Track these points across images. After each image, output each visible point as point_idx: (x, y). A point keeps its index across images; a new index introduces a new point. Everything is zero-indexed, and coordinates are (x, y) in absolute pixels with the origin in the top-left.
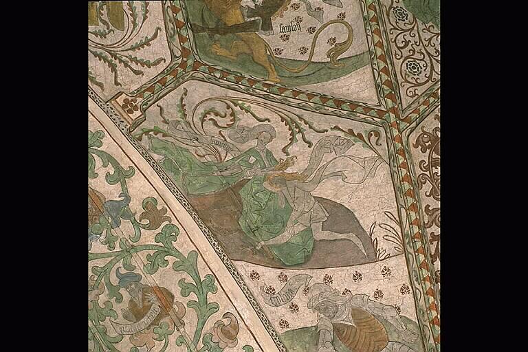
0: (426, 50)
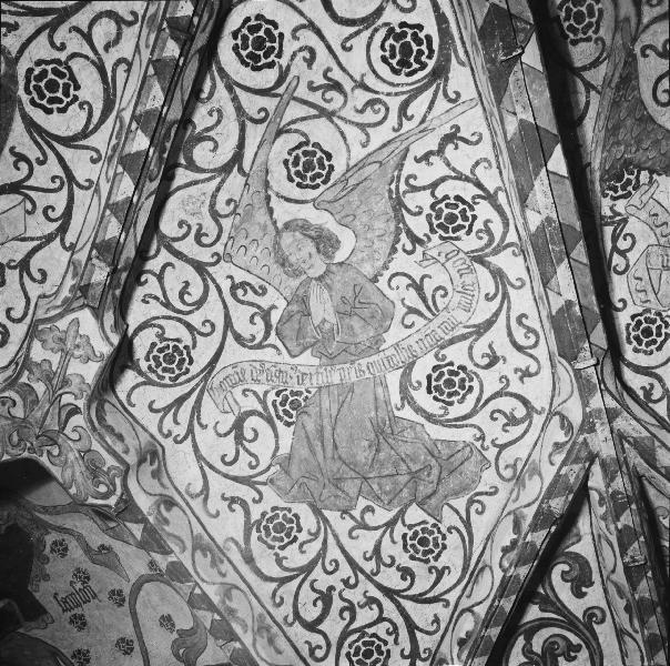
0: (380, 587)
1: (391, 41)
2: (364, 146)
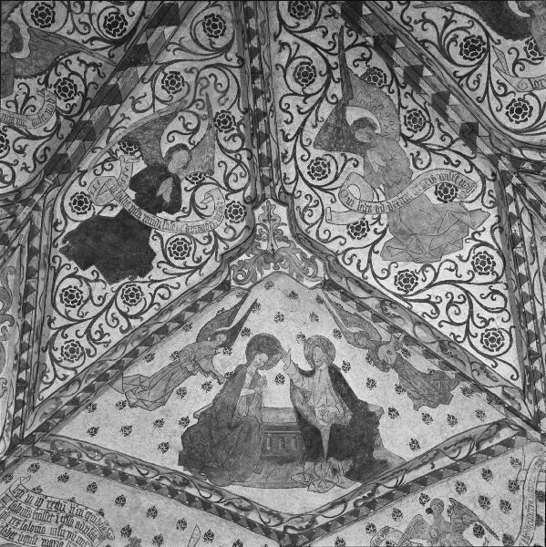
1: (114, 16)
2: (68, 33)
